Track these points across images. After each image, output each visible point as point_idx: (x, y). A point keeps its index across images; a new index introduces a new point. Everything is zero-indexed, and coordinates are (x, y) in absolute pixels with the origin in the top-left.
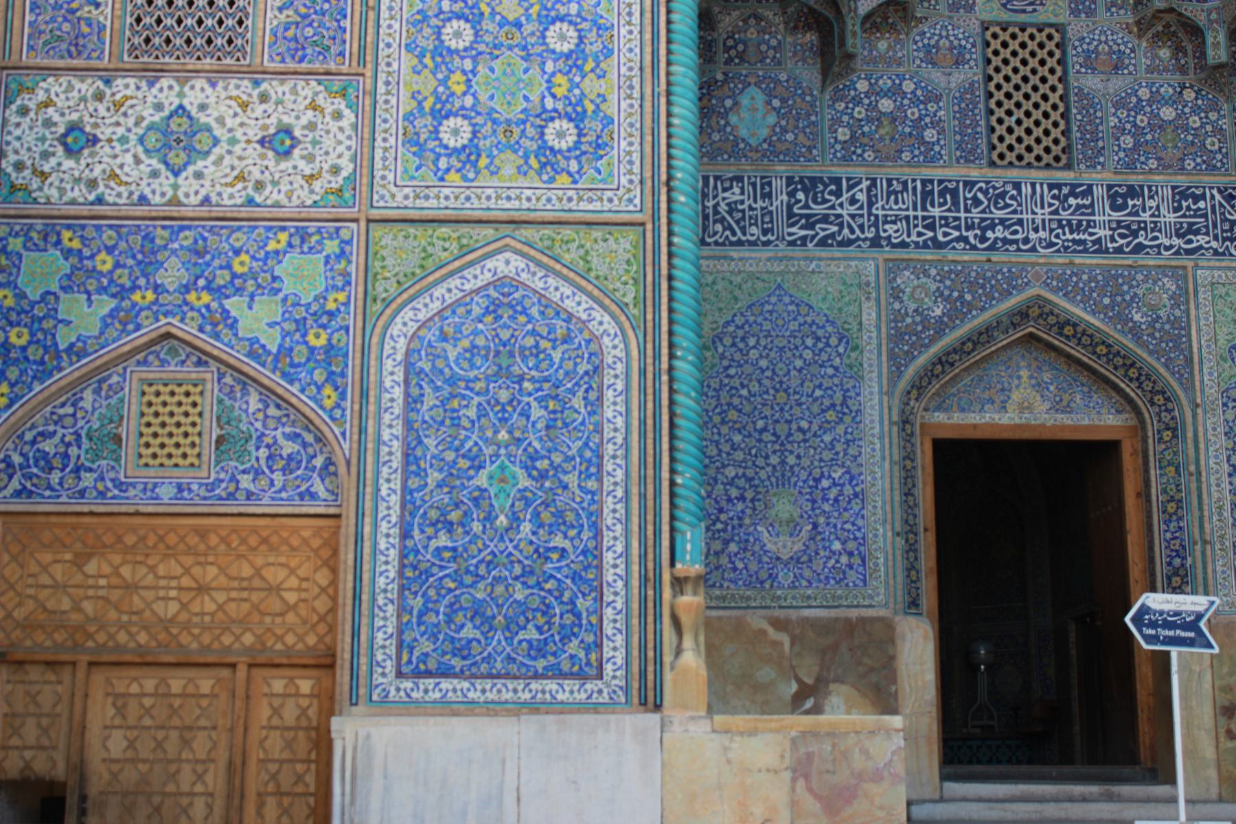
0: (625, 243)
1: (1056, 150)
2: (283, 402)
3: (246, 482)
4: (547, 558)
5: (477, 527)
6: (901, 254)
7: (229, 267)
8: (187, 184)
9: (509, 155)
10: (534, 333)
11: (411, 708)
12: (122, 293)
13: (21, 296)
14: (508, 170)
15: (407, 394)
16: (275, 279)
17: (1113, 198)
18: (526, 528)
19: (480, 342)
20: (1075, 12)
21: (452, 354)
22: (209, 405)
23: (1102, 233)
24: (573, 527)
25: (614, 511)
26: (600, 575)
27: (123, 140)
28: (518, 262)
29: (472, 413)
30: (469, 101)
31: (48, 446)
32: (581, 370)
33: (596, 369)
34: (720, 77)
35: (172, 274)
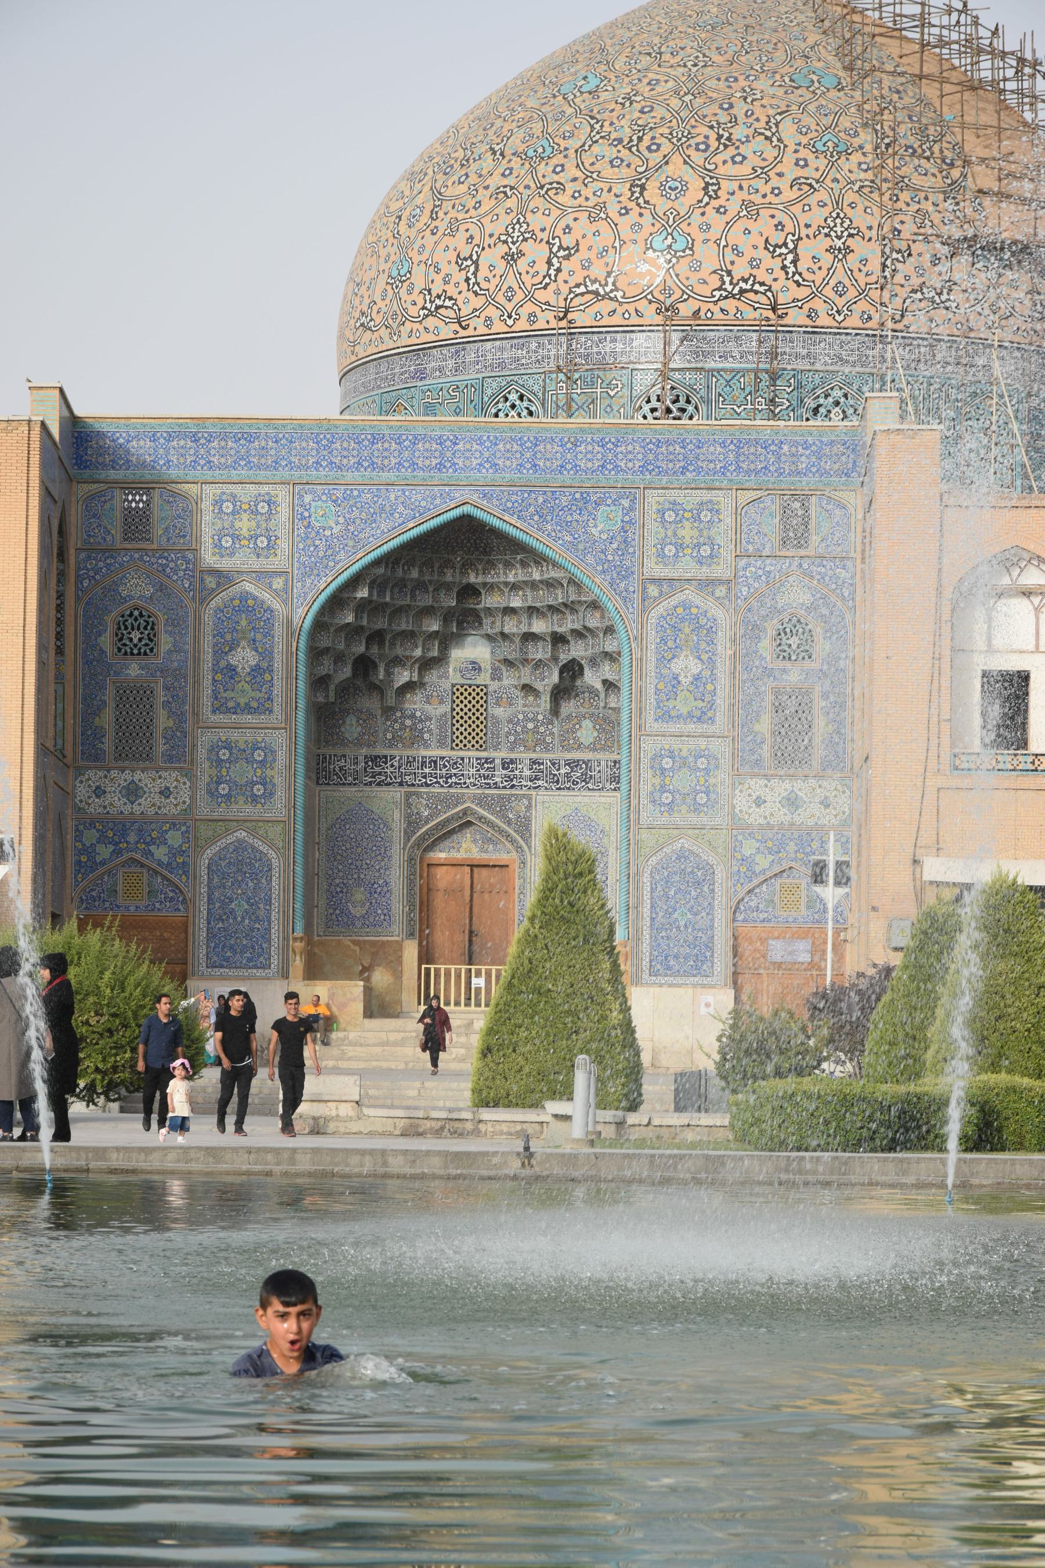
0: (279, 828)
1: (481, 742)
2: (168, 880)
3: (157, 905)
6: (412, 789)
8: (136, 807)
11: (211, 978)
12: (116, 844)
14: (241, 802)
17: (503, 764)
20: (493, 679)
22: (145, 879)
23: (498, 780)
28: (244, 834)
31: (94, 894)
35: (132, 838)
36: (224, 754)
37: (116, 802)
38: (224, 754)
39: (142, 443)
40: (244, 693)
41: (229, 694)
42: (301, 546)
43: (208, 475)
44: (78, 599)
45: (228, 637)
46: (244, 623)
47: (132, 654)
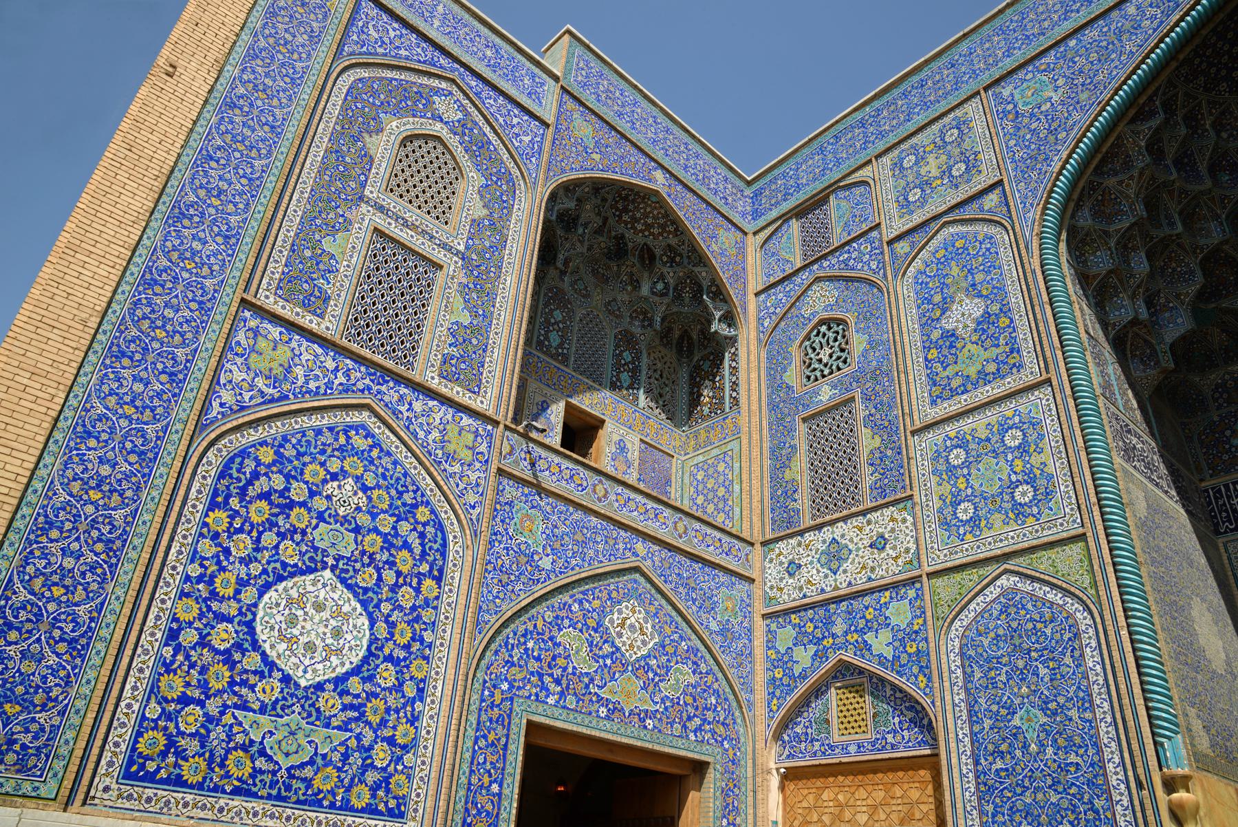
2: (901, 691)
3: (890, 737)
4: (1068, 771)
5: (1018, 753)
7: (864, 617)
8: (841, 577)
9: (997, 515)
10: (1032, 620)
12: (819, 641)
13: (778, 652)
15: (964, 673)
16: (886, 618)
18: (1050, 750)
19: (1001, 632)
21: (986, 643)
24: (1081, 747)
25: (1108, 733)
26: (1107, 781)
27: (811, 563)
29: (1003, 678)
30: (969, 491)
32: (1066, 637)
33: (1075, 635)
34: (1216, 419)
35: (839, 629)
36: (957, 457)
37: (817, 580)
38: (957, 457)
39: (811, 162)
40: (973, 358)
41: (950, 371)
42: (1012, 143)
43: (881, 146)
44: (759, 340)
45: (937, 298)
46: (955, 271)
47: (824, 376)
